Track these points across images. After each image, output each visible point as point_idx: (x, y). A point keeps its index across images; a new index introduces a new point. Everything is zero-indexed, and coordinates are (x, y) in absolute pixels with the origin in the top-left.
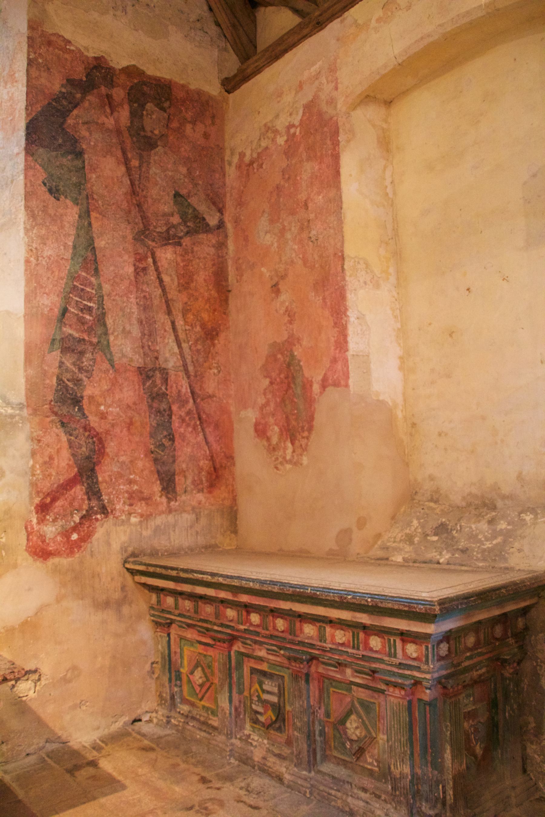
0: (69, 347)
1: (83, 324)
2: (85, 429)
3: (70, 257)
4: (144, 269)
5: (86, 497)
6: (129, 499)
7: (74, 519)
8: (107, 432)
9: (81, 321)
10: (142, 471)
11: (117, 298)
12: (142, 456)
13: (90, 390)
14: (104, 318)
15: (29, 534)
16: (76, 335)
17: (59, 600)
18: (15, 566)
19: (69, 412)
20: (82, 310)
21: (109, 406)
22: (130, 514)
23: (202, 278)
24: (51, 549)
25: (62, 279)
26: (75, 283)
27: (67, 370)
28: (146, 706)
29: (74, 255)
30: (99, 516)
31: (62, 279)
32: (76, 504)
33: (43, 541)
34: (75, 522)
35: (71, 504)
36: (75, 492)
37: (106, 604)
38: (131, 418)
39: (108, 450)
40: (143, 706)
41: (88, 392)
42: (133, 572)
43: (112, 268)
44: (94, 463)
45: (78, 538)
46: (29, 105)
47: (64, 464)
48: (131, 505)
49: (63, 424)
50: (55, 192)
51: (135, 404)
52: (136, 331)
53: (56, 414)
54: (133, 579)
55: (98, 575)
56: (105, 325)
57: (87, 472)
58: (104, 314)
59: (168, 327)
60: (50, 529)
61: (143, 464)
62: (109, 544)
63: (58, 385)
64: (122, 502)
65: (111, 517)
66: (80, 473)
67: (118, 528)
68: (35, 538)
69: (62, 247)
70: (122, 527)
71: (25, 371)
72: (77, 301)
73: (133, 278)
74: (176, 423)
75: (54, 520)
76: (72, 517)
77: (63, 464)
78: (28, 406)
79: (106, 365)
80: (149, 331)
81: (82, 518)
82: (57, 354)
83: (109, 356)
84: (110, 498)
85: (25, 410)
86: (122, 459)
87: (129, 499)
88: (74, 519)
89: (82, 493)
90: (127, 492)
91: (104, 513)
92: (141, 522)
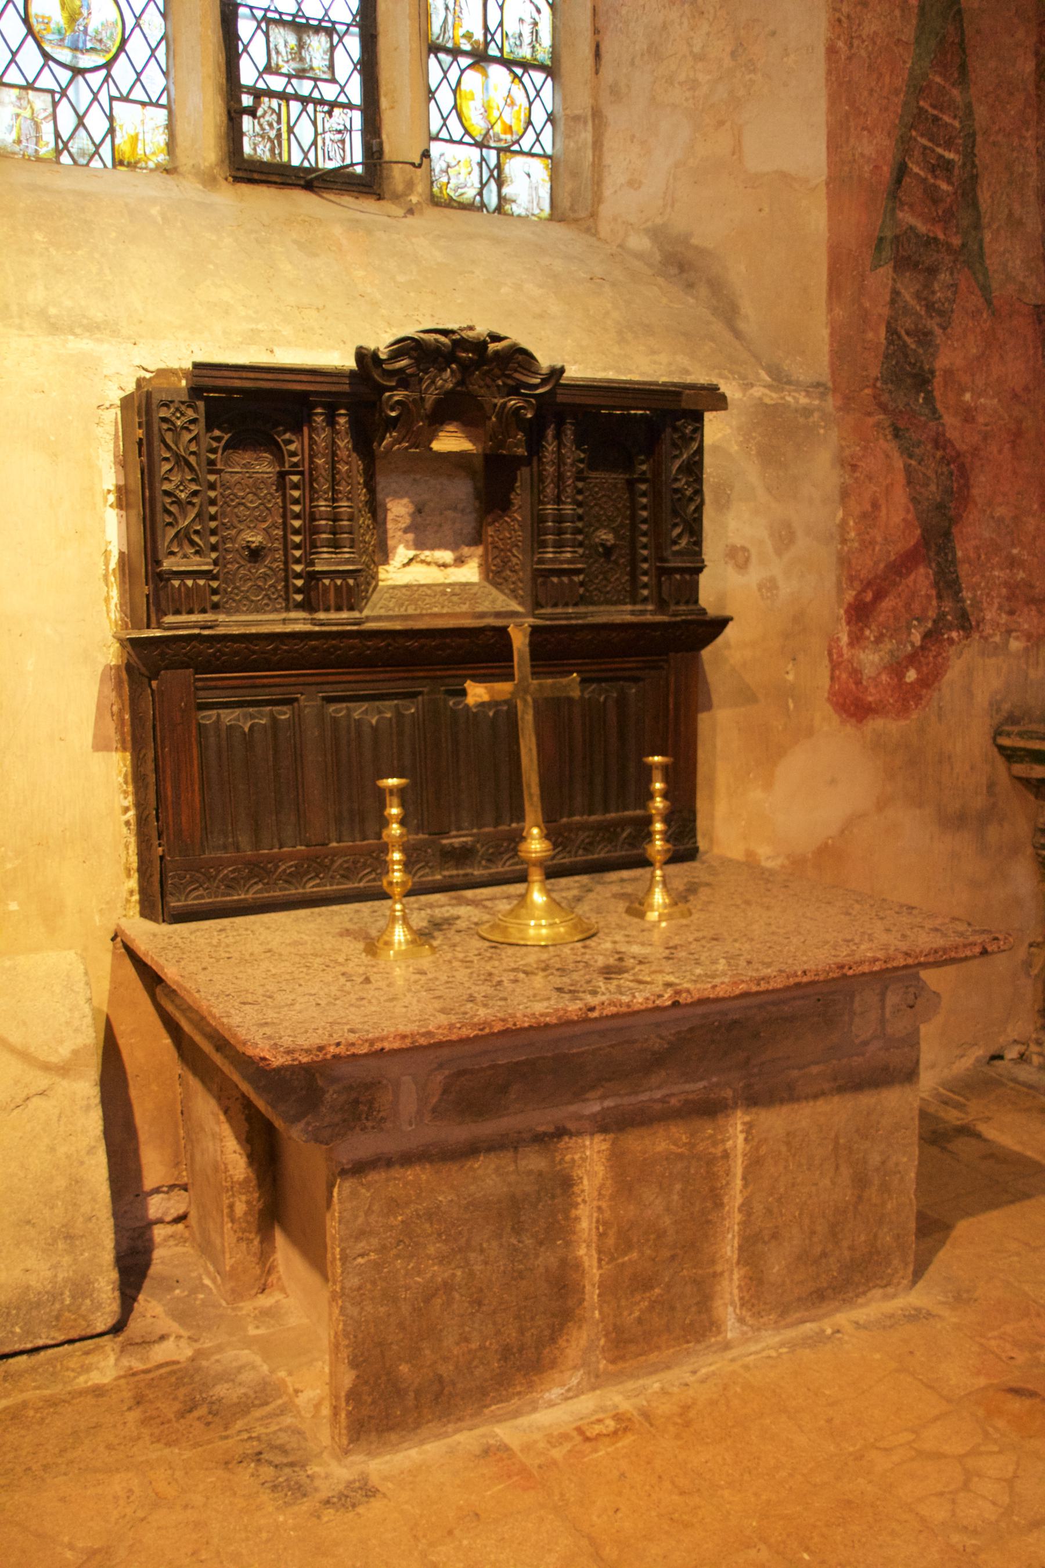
0: (909, 257)
1: (935, 202)
2: (937, 446)
3: (912, 39)
5: (934, 592)
6: (1008, 599)
7: (912, 638)
8: (975, 451)
9: (932, 196)
10: (1034, 538)
11: (1000, 138)
12: (1035, 507)
13: (947, 358)
14: (974, 190)
15: (834, 666)
16: (922, 228)
17: (881, 805)
18: (810, 732)
19: (908, 404)
20: (933, 170)
21: (979, 396)
22: (1009, 632)
24: (870, 699)
25: (897, 92)
26: (922, 103)
27: (906, 311)
28: (1014, 1031)
29: (921, 29)
30: (954, 635)
31: (897, 92)
32: (916, 606)
33: (858, 683)
34: (913, 645)
35: (908, 606)
36: (915, 581)
38: (1019, 422)
39: (975, 491)
40: (1009, 1030)
41: (942, 362)
42: (1010, 755)
43: (992, 64)
44: (950, 520)
45: (917, 680)
48: (1011, 613)
49: (897, 433)
51: (1026, 389)
53: (883, 408)
54: (1009, 769)
55: (950, 757)
56: (974, 204)
57: (936, 538)
58: (974, 178)
60: (871, 657)
62: (970, 694)
63: (890, 342)
64: (996, 605)
65: (976, 636)
66: (925, 540)
67: (987, 660)
68: (844, 676)
69: (897, 13)
70: (993, 660)
71: (830, 310)
72: (925, 148)
73: (1031, 88)
75: (879, 640)
76: (909, 634)
77: (897, 519)
78: (835, 390)
79: (975, 301)
81: (927, 636)
82: (886, 271)
83: (981, 277)
84: (975, 596)
85: (830, 399)
86: (1000, 511)
87: (1008, 599)
88: (912, 638)
89: (927, 583)
90: (1006, 584)
91: (963, 628)
92: (1027, 649)
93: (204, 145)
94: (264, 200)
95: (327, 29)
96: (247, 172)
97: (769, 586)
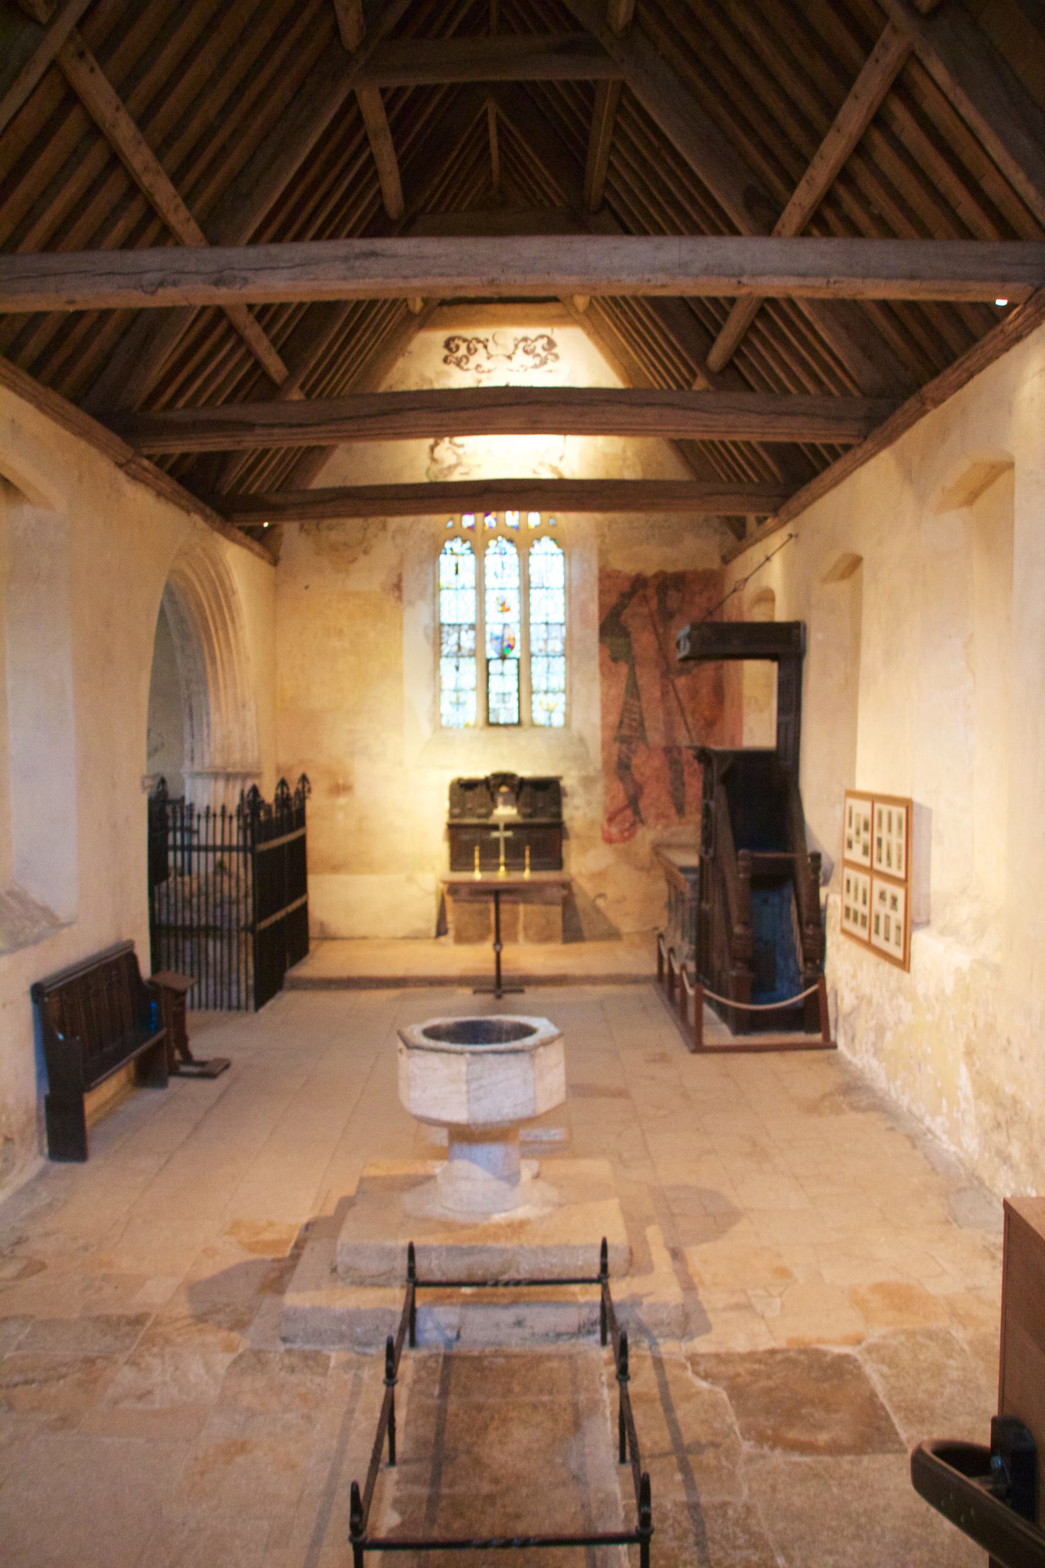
4: (667, 692)
9: (631, 726)
13: (636, 761)
23: (705, 691)
37: (642, 869)
46: (600, 616)
47: (621, 799)
50: (615, 660)
52: (662, 728)
57: (633, 802)
59: (682, 723)
61: (665, 799)
74: (686, 776)
80: (670, 726)
82: (617, 744)
93: (481, 722)
94: (493, 731)
95: (509, 694)
96: (490, 724)
97: (585, 815)
